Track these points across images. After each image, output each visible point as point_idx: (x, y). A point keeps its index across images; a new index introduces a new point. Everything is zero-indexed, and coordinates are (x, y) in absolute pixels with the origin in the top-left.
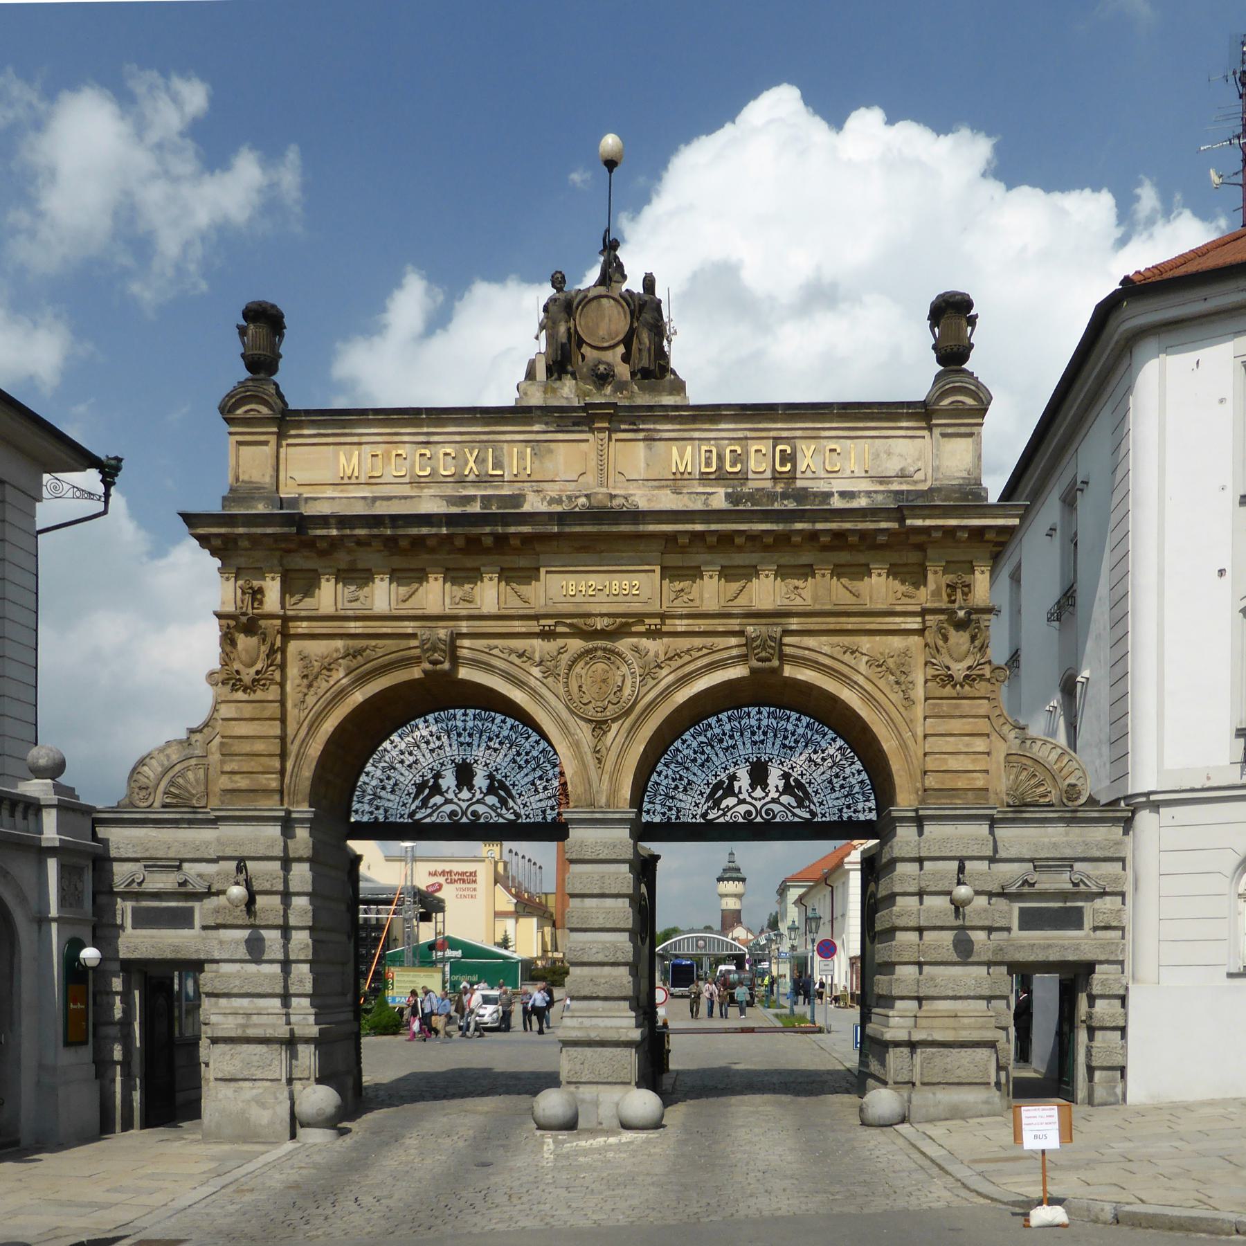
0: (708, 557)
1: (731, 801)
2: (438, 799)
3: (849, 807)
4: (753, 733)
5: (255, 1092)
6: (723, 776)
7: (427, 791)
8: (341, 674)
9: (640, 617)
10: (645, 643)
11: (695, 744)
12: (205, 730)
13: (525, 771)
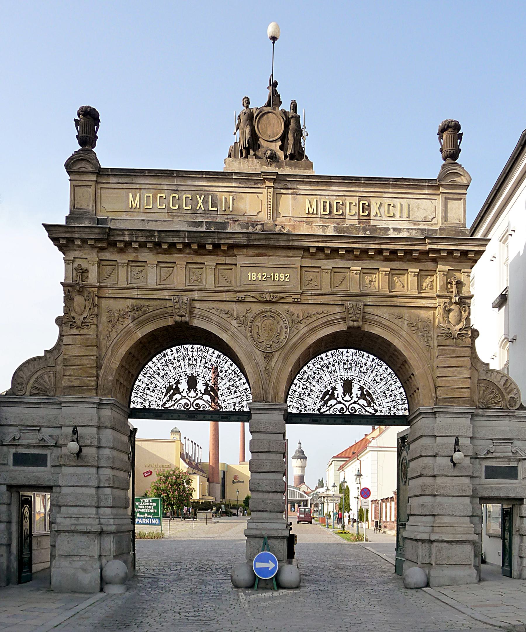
0: (325, 262)
2: (178, 396)
3: (394, 407)
4: (345, 364)
5: (81, 563)
7: (172, 391)
8: (130, 321)
11: (314, 369)
12: (54, 351)
13: (225, 381)
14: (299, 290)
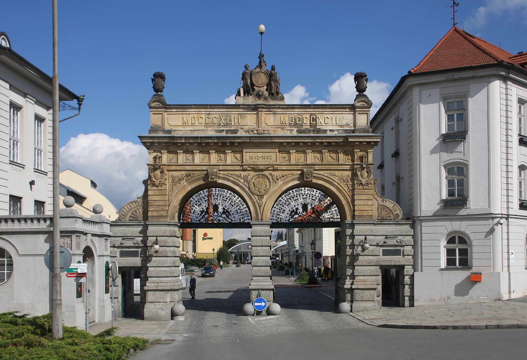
1: (297, 216)
4: (303, 196)
6: (294, 208)
8: (184, 181)
9: (272, 165)
10: (273, 173)
11: (286, 199)
14: (278, 163)
